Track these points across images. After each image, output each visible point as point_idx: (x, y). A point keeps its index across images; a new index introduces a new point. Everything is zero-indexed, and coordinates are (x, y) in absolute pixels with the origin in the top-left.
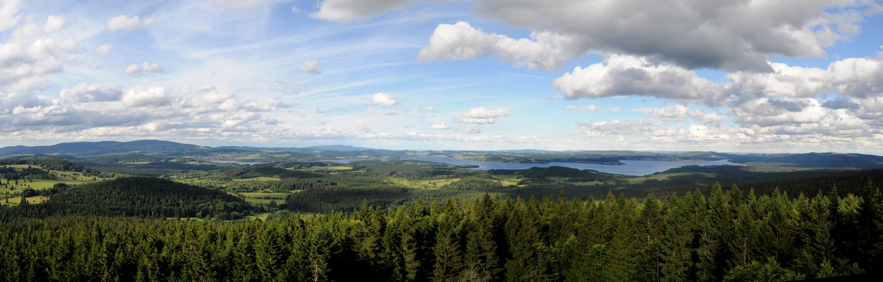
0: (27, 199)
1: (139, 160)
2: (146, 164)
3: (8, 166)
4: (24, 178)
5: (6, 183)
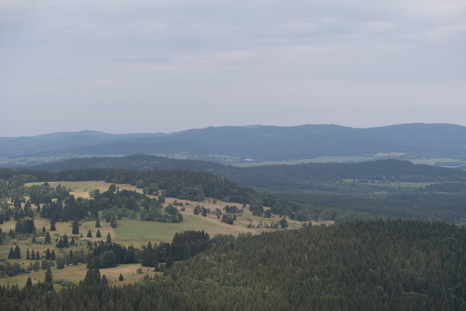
0: (103, 272)
1: (401, 177)
2: (421, 188)
3: (53, 185)
4: (97, 215)
5: (48, 227)
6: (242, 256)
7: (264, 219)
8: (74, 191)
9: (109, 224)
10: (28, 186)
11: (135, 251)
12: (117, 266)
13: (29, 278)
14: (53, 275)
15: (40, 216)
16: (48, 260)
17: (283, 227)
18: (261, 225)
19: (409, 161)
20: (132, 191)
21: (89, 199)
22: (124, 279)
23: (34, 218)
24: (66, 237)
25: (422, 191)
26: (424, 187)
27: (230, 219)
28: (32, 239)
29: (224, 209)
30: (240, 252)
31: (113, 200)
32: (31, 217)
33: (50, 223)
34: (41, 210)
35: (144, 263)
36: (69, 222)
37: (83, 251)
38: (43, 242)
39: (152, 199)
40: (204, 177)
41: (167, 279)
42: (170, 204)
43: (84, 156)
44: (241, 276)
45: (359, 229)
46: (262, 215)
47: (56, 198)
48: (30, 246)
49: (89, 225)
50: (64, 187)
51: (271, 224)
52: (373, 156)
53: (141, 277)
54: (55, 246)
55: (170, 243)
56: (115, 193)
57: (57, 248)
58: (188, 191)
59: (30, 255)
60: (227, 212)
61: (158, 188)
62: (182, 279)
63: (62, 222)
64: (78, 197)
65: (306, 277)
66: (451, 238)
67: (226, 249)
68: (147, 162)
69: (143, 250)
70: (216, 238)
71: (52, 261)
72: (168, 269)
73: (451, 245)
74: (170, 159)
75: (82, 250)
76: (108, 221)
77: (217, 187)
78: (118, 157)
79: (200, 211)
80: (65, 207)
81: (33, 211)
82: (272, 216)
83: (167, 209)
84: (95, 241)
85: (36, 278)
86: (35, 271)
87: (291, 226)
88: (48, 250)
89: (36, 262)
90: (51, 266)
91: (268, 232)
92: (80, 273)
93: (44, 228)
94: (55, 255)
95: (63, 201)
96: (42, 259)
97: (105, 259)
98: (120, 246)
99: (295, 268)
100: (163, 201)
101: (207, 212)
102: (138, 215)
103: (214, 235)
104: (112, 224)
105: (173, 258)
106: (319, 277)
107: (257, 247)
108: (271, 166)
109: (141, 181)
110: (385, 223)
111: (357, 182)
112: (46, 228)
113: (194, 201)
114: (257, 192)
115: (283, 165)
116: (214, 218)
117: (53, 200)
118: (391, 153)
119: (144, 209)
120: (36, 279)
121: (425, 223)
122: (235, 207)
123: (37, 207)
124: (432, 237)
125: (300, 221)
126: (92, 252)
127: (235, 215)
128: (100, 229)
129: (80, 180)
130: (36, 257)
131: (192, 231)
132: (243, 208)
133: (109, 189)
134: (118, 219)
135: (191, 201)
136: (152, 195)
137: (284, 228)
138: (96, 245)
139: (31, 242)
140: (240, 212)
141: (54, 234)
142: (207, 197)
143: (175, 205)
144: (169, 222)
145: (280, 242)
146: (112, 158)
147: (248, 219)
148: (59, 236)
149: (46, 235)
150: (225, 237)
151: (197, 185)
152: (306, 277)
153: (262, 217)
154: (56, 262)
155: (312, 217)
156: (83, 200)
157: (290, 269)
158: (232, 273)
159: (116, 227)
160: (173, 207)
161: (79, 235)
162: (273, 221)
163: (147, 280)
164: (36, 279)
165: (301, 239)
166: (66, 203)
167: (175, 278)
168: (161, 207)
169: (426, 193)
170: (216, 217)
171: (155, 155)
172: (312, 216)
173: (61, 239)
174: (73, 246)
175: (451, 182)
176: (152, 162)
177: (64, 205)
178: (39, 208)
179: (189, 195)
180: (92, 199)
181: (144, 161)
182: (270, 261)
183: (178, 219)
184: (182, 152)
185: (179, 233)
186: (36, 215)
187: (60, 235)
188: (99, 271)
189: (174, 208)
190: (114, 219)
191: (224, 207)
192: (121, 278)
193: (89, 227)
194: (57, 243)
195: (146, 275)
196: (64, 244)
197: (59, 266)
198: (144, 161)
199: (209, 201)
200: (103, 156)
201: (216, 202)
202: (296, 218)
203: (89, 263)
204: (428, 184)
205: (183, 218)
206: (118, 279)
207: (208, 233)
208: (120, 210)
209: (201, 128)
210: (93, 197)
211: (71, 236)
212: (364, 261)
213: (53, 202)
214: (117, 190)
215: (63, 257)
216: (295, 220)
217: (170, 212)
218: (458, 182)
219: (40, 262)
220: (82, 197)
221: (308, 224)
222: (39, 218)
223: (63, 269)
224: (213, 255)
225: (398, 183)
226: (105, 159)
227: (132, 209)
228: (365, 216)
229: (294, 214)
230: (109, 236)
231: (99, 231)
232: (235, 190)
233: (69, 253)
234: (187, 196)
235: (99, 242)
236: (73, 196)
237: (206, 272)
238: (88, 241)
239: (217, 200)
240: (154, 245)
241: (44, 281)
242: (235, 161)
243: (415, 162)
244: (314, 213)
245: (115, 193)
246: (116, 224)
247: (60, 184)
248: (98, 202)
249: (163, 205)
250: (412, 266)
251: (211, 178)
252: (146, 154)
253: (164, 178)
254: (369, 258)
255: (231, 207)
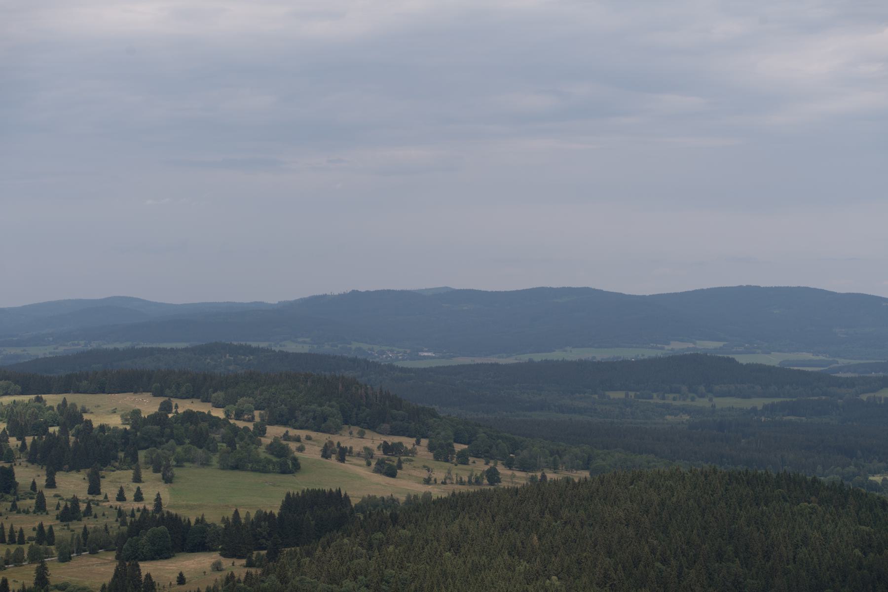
0: (146, 568)
2: (754, 410)
3: (52, 400)
4: (135, 459)
5: (42, 481)
6: (413, 537)
7: (456, 467)
8: (92, 413)
9: (159, 475)
10: (3, 403)
11: (208, 528)
12: (173, 556)
13: (3, 579)
14: (50, 574)
15: (27, 461)
16: (41, 545)
17: (491, 484)
18: (450, 479)
19: (732, 358)
20: (203, 412)
21: (121, 427)
22: (187, 580)
23: (15, 465)
24: (75, 501)
25: (756, 415)
26: (760, 408)
27: (391, 467)
28: (10, 504)
29: (379, 448)
30: (410, 531)
31: (166, 429)
32: (9, 462)
33: (46, 473)
34: (29, 448)
35: (225, 550)
36: (82, 471)
37: (109, 527)
38: (31, 510)
39: (242, 428)
40: (340, 387)
41: (270, 583)
42: (276, 439)
43: (111, 346)
44: (411, 576)
45: (636, 487)
46: (452, 459)
47: (58, 425)
48: (5, 517)
49: (120, 478)
50: (74, 405)
51: (468, 477)
52: (663, 349)
53: (219, 578)
54: (55, 517)
55: (276, 512)
56: (170, 416)
57: (58, 522)
58: (311, 414)
59: (6, 535)
60: (385, 453)
61: (253, 407)
62: (298, 581)
63: (67, 472)
64: (100, 424)
65: (535, 579)
66: (811, 504)
67: (383, 524)
68: (232, 358)
69: (223, 526)
70: (364, 504)
71: (48, 547)
72: (271, 563)
73: (811, 517)
74: (277, 351)
75: (106, 526)
76: (156, 471)
77: (366, 406)
78: (177, 349)
79: (333, 452)
80: (74, 442)
81: (12, 451)
82: (470, 462)
83: (271, 448)
84: (132, 508)
85: (17, 580)
86: (16, 566)
87: (507, 480)
88: (41, 526)
89: (17, 549)
90: (47, 556)
91: (463, 493)
92: (103, 569)
93: (34, 483)
94: (55, 534)
95: (70, 432)
96: (29, 542)
97: (151, 543)
98: (180, 518)
99: (514, 560)
100: (263, 432)
101: (347, 454)
102: (215, 459)
103: (360, 498)
104: (164, 475)
105: (281, 542)
106: (559, 579)
107: (441, 521)
108: (470, 365)
109: (220, 395)
110: (686, 475)
111: (633, 397)
112: (37, 484)
113: (321, 432)
114: (442, 415)
115: (492, 365)
116: (360, 466)
117: (51, 430)
118: (698, 342)
119: (227, 446)
120: (17, 582)
121: (762, 474)
122: (400, 444)
123: (19, 443)
124: (774, 501)
125: (524, 471)
126: (125, 529)
127: (399, 459)
128: (140, 485)
129: (104, 392)
130: (17, 538)
131: (317, 489)
132: (416, 446)
133: (160, 409)
134: (177, 466)
135: (316, 433)
136: (241, 420)
137: (493, 485)
138: (133, 515)
139: (9, 509)
140: (410, 455)
141: (52, 496)
142: (346, 424)
143: (285, 440)
144: (274, 472)
145: (485, 512)
146: (165, 349)
147: (424, 467)
148: (62, 499)
149: (38, 497)
150: (382, 502)
151: (328, 403)
152: (535, 579)
153: (452, 463)
154: (57, 548)
155: (546, 464)
156: (109, 429)
157: (504, 563)
158: (394, 570)
159: (173, 481)
160: (282, 444)
161: (101, 498)
162: (472, 471)
163: (231, 583)
164: (17, 582)
165: (526, 505)
166: (76, 435)
167: (284, 580)
168: (260, 443)
169: (763, 419)
170: (364, 462)
171: (248, 343)
172: (547, 462)
173: (66, 504)
174: (88, 519)
175: (811, 398)
176: (243, 357)
177: (72, 439)
178: (24, 445)
179: (313, 421)
180: (126, 429)
181: (228, 355)
182: (466, 549)
183: (291, 466)
184: (300, 340)
185: (294, 494)
186: (18, 458)
187: (65, 497)
188: (138, 566)
189: (284, 445)
190: (168, 467)
191: (379, 444)
192: (181, 580)
193: (120, 482)
194: (58, 512)
195: (230, 573)
196: (73, 513)
197: (62, 557)
198: (228, 355)
199: (351, 433)
200: (148, 346)
201: (363, 435)
202: (516, 466)
203: (120, 550)
204: (768, 401)
205: (301, 465)
206: (175, 582)
207: (349, 493)
208: (179, 449)
209: (336, 293)
210: (128, 424)
211: (85, 498)
212: (647, 549)
213: (52, 433)
214: (175, 410)
215: (70, 540)
216: (514, 469)
217: (275, 453)
218: (824, 398)
219: (26, 548)
220: (107, 423)
221: (539, 478)
222: (24, 464)
223: (69, 561)
224: (358, 535)
225: (711, 400)
226: (150, 352)
227: (204, 448)
228: (649, 462)
229: (512, 457)
230: (158, 500)
231: (138, 489)
232: (400, 411)
233: (81, 531)
234: (309, 422)
235: (138, 510)
236: (89, 423)
237: (345, 569)
238: (118, 508)
239: (366, 431)
240: (245, 516)
241: (33, 585)
242: (400, 356)
243: (743, 359)
244: (551, 456)
245: (170, 416)
246: (173, 476)
247: (65, 398)
248: (138, 434)
249: (263, 439)
250: (736, 557)
251: (354, 388)
252: (231, 343)
253: (264, 388)
254: (655, 542)
255: (393, 444)
